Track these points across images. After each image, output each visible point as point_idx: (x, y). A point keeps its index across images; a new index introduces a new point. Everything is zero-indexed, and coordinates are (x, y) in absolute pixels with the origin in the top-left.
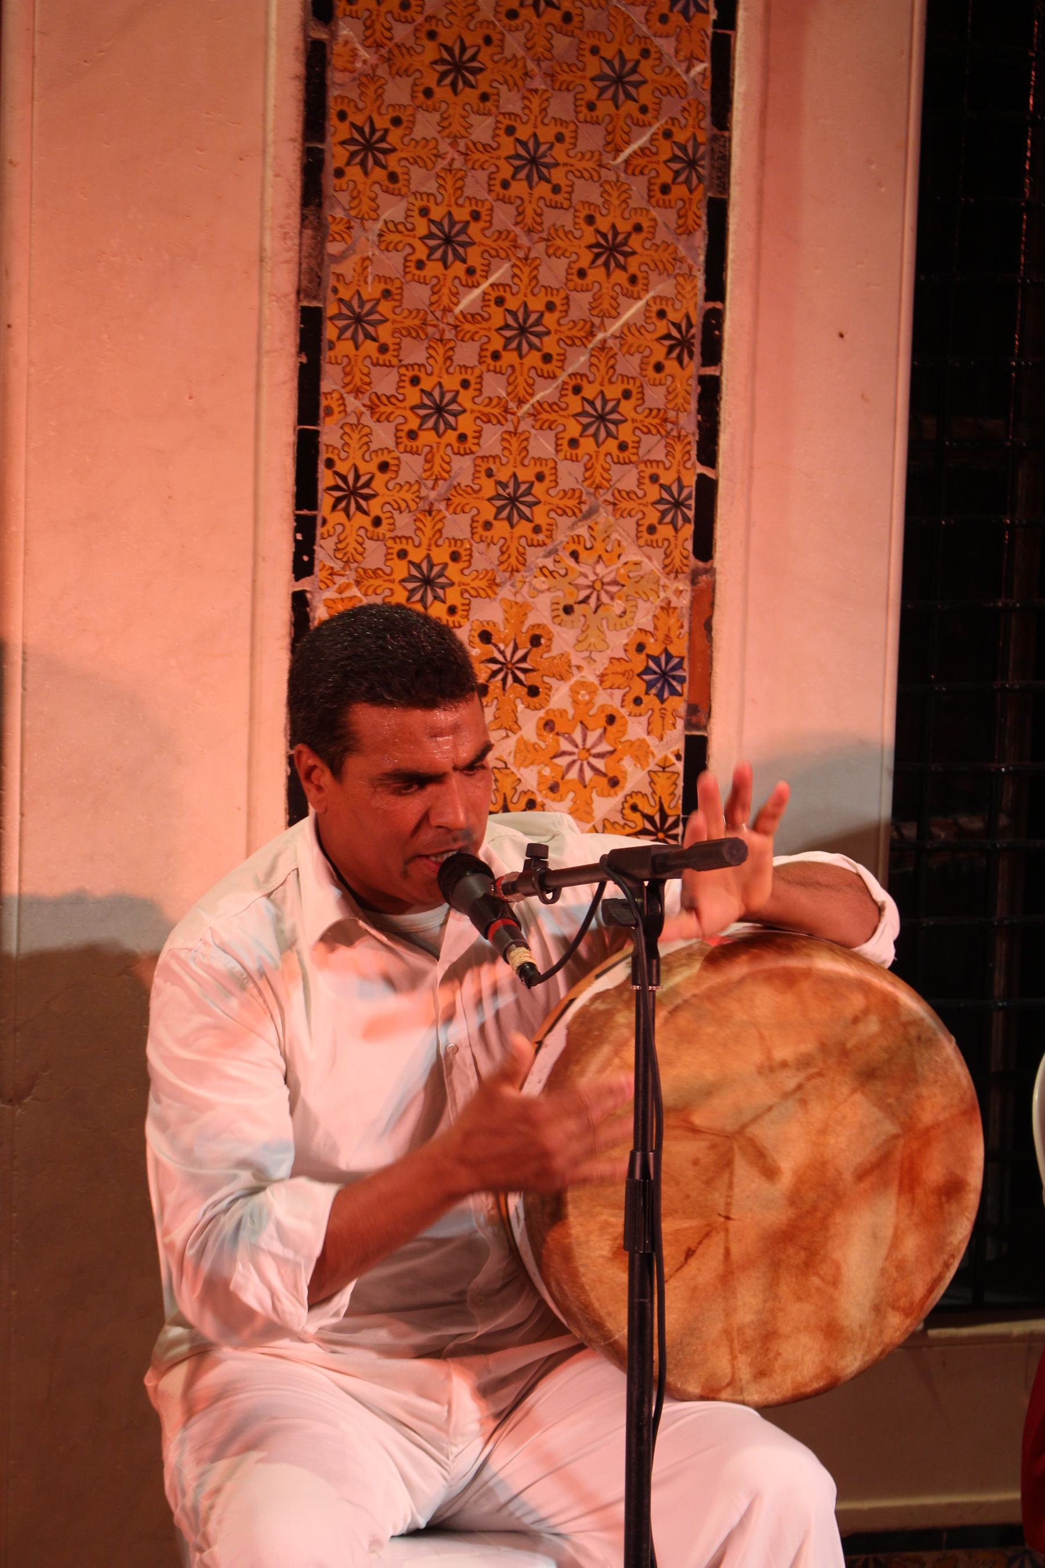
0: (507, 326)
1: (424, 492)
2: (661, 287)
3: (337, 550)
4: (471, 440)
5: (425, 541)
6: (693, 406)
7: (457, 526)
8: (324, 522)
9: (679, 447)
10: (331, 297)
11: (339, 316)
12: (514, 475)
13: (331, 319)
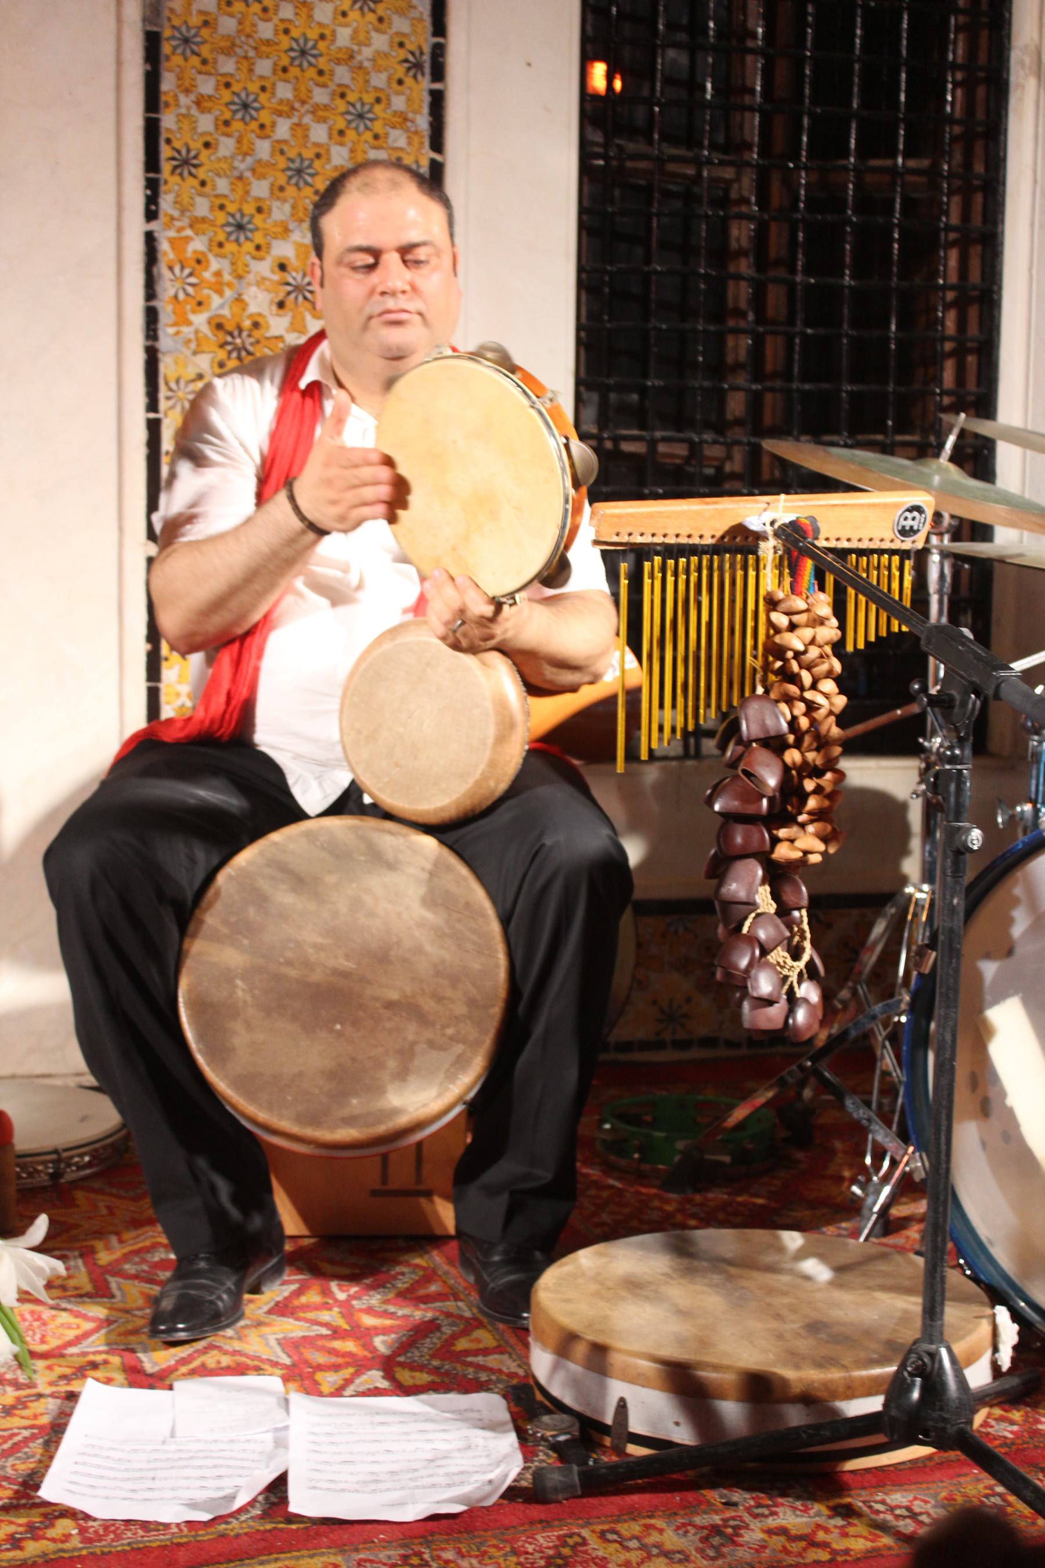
0: (292, 49)
1: (236, 164)
2: (400, 25)
3: (176, 202)
4: (268, 129)
5: (238, 198)
6: (426, 110)
7: (260, 189)
8: (166, 182)
9: (416, 139)
10: (166, 24)
11: (173, 38)
12: (300, 155)
13: (168, 39)
